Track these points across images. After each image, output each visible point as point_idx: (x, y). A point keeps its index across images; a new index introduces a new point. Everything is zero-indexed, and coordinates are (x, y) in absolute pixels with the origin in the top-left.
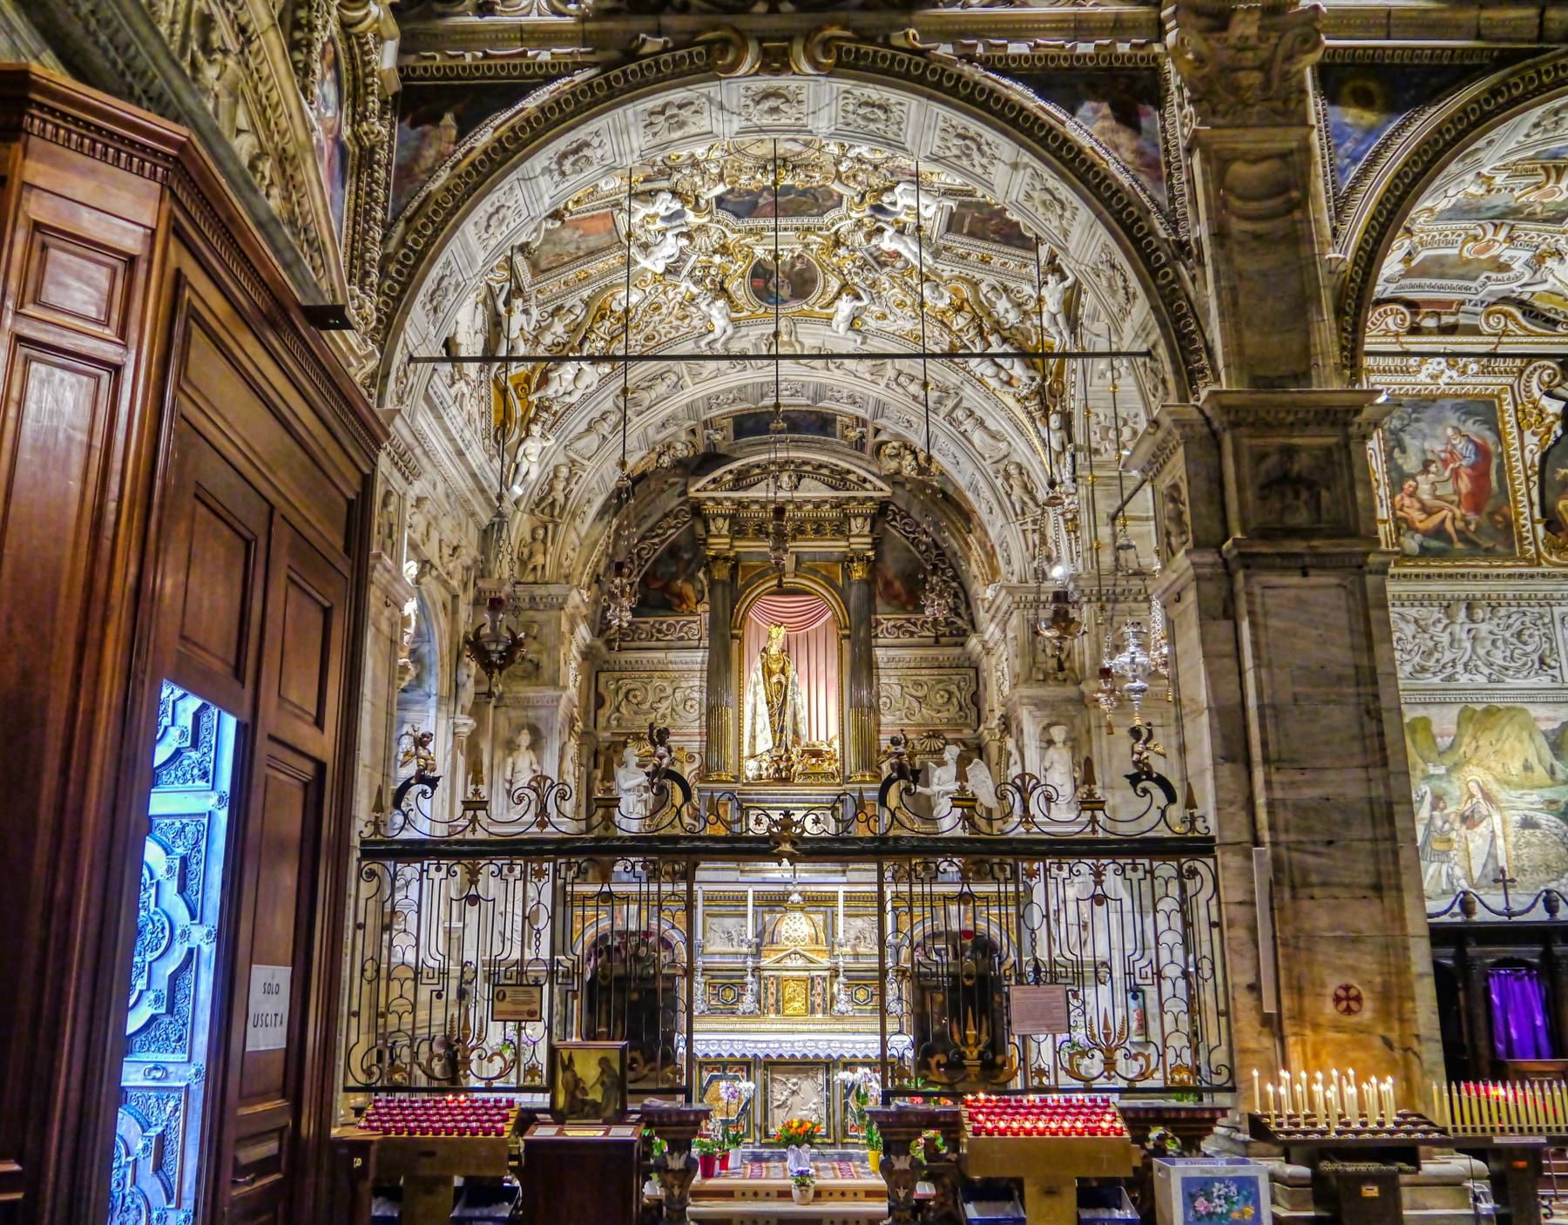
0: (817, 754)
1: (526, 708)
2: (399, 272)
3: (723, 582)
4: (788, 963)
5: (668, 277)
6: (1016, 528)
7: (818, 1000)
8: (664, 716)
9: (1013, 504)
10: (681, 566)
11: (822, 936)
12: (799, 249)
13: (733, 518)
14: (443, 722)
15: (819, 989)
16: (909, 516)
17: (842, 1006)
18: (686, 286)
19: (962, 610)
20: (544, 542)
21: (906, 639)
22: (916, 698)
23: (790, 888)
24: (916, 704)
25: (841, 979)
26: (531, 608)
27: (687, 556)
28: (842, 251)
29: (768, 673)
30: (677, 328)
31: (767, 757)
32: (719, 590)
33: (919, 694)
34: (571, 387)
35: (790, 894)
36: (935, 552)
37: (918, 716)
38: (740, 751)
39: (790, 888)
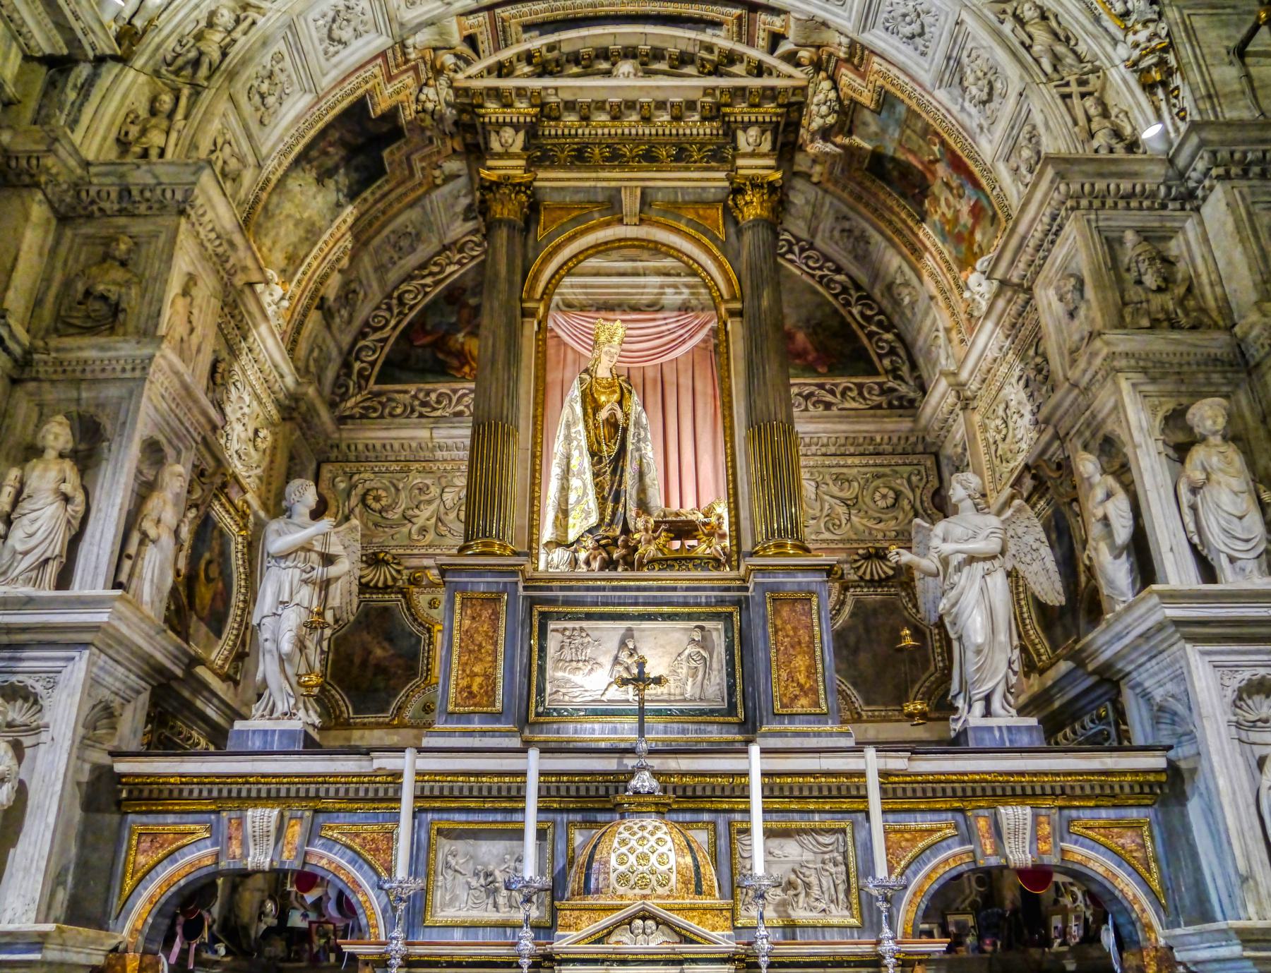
0: (683, 530)
1: (77, 383)
3: (511, 225)
4: (624, 942)
6: (1050, 92)
8: (423, 530)
9: (1037, 61)
10: (465, 313)
11: (709, 871)
13: (531, 131)
16: (812, 246)
20: (171, 115)
22: (843, 500)
23: (630, 762)
24: (841, 510)
26: (122, 212)
31: (589, 542)
32: (502, 235)
33: (846, 494)
35: (632, 774)
36: (855, 294)
37: (846, 528)
38: (533, 525)
39: (630, 762)
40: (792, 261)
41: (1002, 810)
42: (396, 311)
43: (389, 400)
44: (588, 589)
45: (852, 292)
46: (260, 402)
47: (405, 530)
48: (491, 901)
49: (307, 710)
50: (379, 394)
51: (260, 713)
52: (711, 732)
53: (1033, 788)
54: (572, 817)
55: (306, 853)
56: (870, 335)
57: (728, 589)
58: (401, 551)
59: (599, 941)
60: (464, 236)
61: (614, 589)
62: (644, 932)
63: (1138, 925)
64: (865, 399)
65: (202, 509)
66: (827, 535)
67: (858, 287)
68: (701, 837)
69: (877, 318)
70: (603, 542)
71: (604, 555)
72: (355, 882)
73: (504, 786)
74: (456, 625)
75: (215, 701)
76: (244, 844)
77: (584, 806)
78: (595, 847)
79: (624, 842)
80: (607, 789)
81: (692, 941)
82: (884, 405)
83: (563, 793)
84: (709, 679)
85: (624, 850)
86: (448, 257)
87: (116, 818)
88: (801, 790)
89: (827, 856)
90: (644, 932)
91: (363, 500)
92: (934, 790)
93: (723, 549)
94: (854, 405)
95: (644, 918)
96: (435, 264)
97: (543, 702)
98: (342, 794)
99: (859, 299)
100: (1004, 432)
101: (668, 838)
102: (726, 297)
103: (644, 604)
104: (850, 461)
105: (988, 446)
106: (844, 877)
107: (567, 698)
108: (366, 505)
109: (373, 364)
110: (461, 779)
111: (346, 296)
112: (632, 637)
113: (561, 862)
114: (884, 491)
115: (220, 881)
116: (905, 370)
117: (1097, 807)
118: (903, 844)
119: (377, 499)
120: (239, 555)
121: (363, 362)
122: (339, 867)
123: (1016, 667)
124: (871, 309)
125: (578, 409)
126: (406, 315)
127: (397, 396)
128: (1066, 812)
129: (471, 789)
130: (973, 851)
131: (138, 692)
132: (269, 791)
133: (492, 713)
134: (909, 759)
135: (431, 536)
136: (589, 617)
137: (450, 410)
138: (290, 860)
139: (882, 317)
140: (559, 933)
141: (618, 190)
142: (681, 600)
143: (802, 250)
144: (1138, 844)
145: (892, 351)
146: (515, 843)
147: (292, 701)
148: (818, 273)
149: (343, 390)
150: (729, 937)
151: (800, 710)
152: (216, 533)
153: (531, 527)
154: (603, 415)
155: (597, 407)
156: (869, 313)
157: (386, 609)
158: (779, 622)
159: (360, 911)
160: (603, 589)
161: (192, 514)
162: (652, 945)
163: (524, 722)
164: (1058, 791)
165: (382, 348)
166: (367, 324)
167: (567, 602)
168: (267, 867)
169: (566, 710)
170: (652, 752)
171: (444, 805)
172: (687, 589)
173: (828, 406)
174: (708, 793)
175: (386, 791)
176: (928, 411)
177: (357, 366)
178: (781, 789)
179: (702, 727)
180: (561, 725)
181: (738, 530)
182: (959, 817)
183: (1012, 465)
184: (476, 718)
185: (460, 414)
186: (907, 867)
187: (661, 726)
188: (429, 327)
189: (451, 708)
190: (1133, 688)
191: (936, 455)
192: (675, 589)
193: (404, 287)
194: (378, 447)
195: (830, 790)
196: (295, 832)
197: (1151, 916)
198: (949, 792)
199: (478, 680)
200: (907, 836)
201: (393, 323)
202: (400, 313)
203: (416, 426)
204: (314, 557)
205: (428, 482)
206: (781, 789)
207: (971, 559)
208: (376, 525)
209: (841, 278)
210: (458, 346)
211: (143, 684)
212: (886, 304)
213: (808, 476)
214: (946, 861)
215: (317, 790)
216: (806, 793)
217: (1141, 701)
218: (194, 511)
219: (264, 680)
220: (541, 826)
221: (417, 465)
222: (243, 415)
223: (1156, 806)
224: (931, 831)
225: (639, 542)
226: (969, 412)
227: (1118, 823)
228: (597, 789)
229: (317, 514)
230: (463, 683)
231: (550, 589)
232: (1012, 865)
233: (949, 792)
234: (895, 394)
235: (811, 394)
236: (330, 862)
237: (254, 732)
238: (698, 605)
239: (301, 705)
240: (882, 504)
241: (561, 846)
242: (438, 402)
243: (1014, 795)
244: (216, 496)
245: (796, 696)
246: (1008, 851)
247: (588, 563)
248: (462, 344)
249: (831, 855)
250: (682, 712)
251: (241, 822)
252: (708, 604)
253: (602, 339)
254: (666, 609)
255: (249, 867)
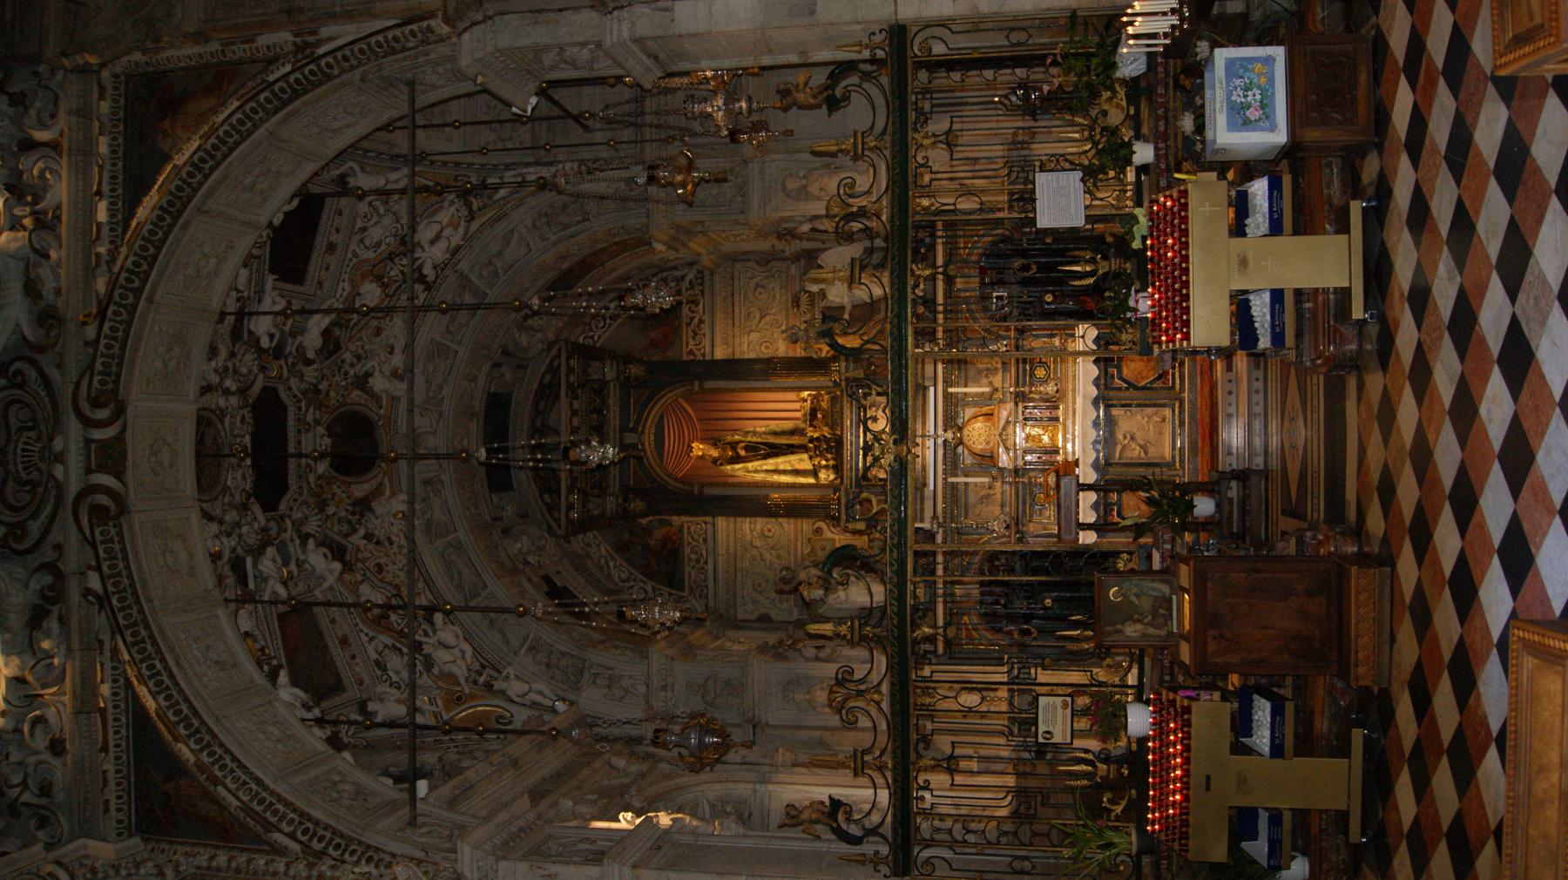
0: (813, 413)
2: (321, 839)
5: (348, 558)
8: (778, 557)
12: (320, 430)
14: (781, 777)
17: (1050, 388)
18: (357, 539)
21: (706, 328)
23: (940, 441)
24: (768, 318)
25: (1027, 389)
27: (627, 536)
28: (323, 386)
29: (737, 459)
30: (401, 547)
33: (758, 316)
34: (456, 651)
38: (810, 486)
40: (599, 337)
96: (599, 561)
109: (670, 594)
125: (737, 466)
143: (591, 330)
202: (635, 580)
235: (694, 331)
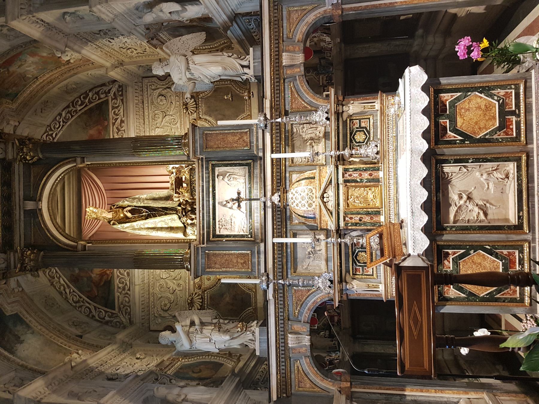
0: (179, 182)
4: (331, 205)
7: (366, 175)
11: (307, 174)
15: (355, 175)
16: (49, 126)
19: (106, 89)
23: (269, 204)
24: (167, 118)
29: (126, 220)
31: (184, 219)
33: (161, 117)
35: (273, 203)
37: (175, 116)
38: (177, 241)
39: (269, 204)
41: (284, 64)
42: (82, 304)
43: (122, 304)
44: (203, 219)
45: (70, 109)
46: (125, 358)
47: (178, 292)
48: (318, 252)
49: (252, 326)
50: (120, 309)
51: (253, 345)
52: (257, 173)
53: (276, 51)
54: (288, 224)
55: (304, 322)
56: (90, 102)
57: (202, 165)
58: (187, 293)
59: (331, 213)
60: (46, 276)
61: (203, 209)
62: (328, 197)
63: (324, 15)
64: (119, 106)
65: (171, 377)
66: (178, 124)
67: (68, 107)
68: (295, 177)
69: (82, 99)
70: (184, 214)
71: (189, 213)
72: (313, 303)
73: (278, 249)
74: (218, 270)
75: (248, 363)
76: (301, 347)
77: (284, 219)
78: (299, 215)
79: (297, 205)
80: (278, 211)
81: (331, 180)
82: (122, 98)
83: (280, 227)
84: (237, 173)
85: (300, 205)
86: (57, 283)
87: (293, 397)
88: (277, 140)
89: (301, 131)
90: (328, 197)
91: (166, 311)
92: (277, 90)
93: (186, 167)
94: (122, 110)
95: (323, 198)
96: (60, 288)
97: (247, 235)
98: (282, 310)
99: (74, 107)
100: (133, 50)
101: (295, 189)
102: (75, 164)
103: (209, 198)
104: (146, 114)
105: (139, 57)
106: (308, 125)
107: (245, 226)
108: (168, 310)
109: (106, 312)
110: (276, 265)
111: (76, 326)
112: (222, 202)
113: (305, 227)
114: (159, 100)
115: (315, 354)
116: (106, 89)
117: (282, 27)
118: (296, 102)
119: (165, 305)
120: (189, 360)
121: (105, 316)
122: (308, 309)
123: (230, 54)
124: (78, 101)
126: (83, 299)
127: (120, 301)
128: (284, 39)
129: (279, 261)
130: (299, 76)
131: (246, 394)
132: (282, 339)
133: (251, 255)
134: (266, 99)
135: (181, 282)
136: (214, 219)
137: (127, 278)
138: (306, 328)
139: (82, 97)
140: (329, 228)
141: (25, 211)
142: (207, 183)
143: (51, 130)
144: (296, 13)
145: (97, 93)
146: (298, 244)
147: (248, 333)
148: (61, 123)
149: (118, 323)
150: (329, 167)
151: (249, 139)
152: (181, 371)
153: (178, 242)
154: (129, 215)
155: (126, 217)
156: (80, 102)
157: (211, 297)
158: (215, 146)
159: (324, 301)
160: (203, 214)
161: (173, 381)
162: (332, 195)
163: (254, 242)
164: (277, 41)
165: (99, 308)
166: (88, 316)
167: (208, 227)
168: (309, 337)
169: (250, 226)
170: (265, 196)
171: (285, 271)
172: (203, 181)
173: (122, 121)
174: (279, 174)
175: (280, 293)
176: (123, 80)
177: (107, 318)
178: (277, 147)
179: (255, 176)
180: (255, 228)
181: (178, 161)
182: (286, 81)
183: (147, 48)
184: (253, 260)
185: (128, 274)
186: (304, 101)
187: (255, 191)
188: (89, 289)
189: (250, 270)
190: (238, 9)
191: (143, 77)
192: (203, 186)
193: (71, 301)
194: (143, 307)
195: (277, 129)
196: (297, 327)
197: (322, 10)
198: (278, 84)
199: (239, 260)
200: (293, 101)
201: (88, 305)
203: (134, 292)
204: (192, 329)
205: (158, 284)
206: (277, 147)
207: (188, 69)
208: (177, 304)
209: (64, 114)
210: (98, 276)
211: (242, 393)
212: (76, 95)
213: (153, 131)
214: (302, 86)
215: (281, 320)
216: (279, 138)
217: (242, 6)
218: (172, 381)
219: (240, 345)
220: (292, 235)
221: (151, 290)
222: (130, 365)
223: (282, 4)
224: (292, 91)
225: (184, 200)
226: (124, 64)
227: (288, 20)
228: (278, 214)
229: (174, 331)
230: (240, 266)
231: (203, 234)
232: (303, 61)
233: (278, 84)
234: (116, 93)
235: (117, 128)
236: (307, 313)
237: (260, 347)
238: (209, 177)
239: (250, 329)
240: (165, 102)
241: (299, 227)
242: (123, 283)
243: (278, 59)
244: (165, 373)
245: (243, 141)
246: (299, 63)
247: (192, 219)
248: (97, 274)
249: (300, 129)
250: (250, 183)
251: (293, 348)
252: (209, 173)
253: (95, 216)
254: (211, 190)
255: (310, 344)
